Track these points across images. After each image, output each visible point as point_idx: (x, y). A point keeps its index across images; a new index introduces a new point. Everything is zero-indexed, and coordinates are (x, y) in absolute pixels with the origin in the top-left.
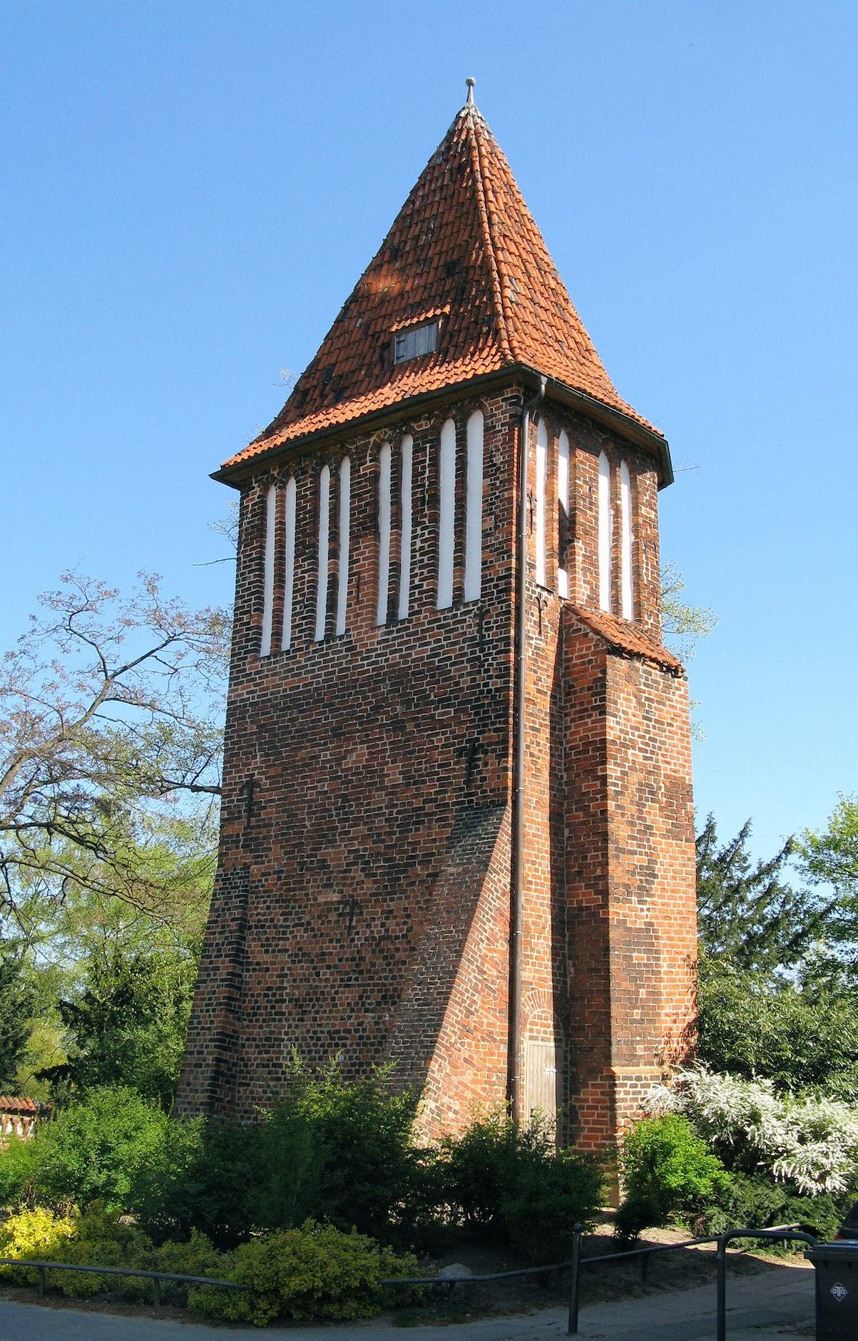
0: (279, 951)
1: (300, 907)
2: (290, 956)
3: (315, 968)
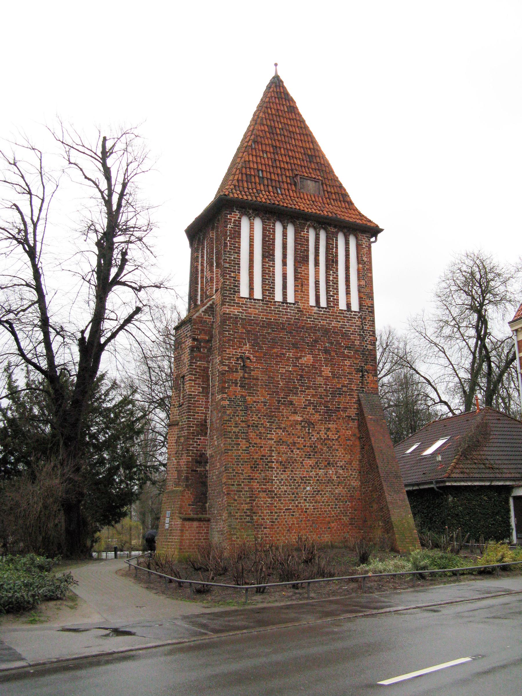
0: (268, 439)
3: (290, 449)
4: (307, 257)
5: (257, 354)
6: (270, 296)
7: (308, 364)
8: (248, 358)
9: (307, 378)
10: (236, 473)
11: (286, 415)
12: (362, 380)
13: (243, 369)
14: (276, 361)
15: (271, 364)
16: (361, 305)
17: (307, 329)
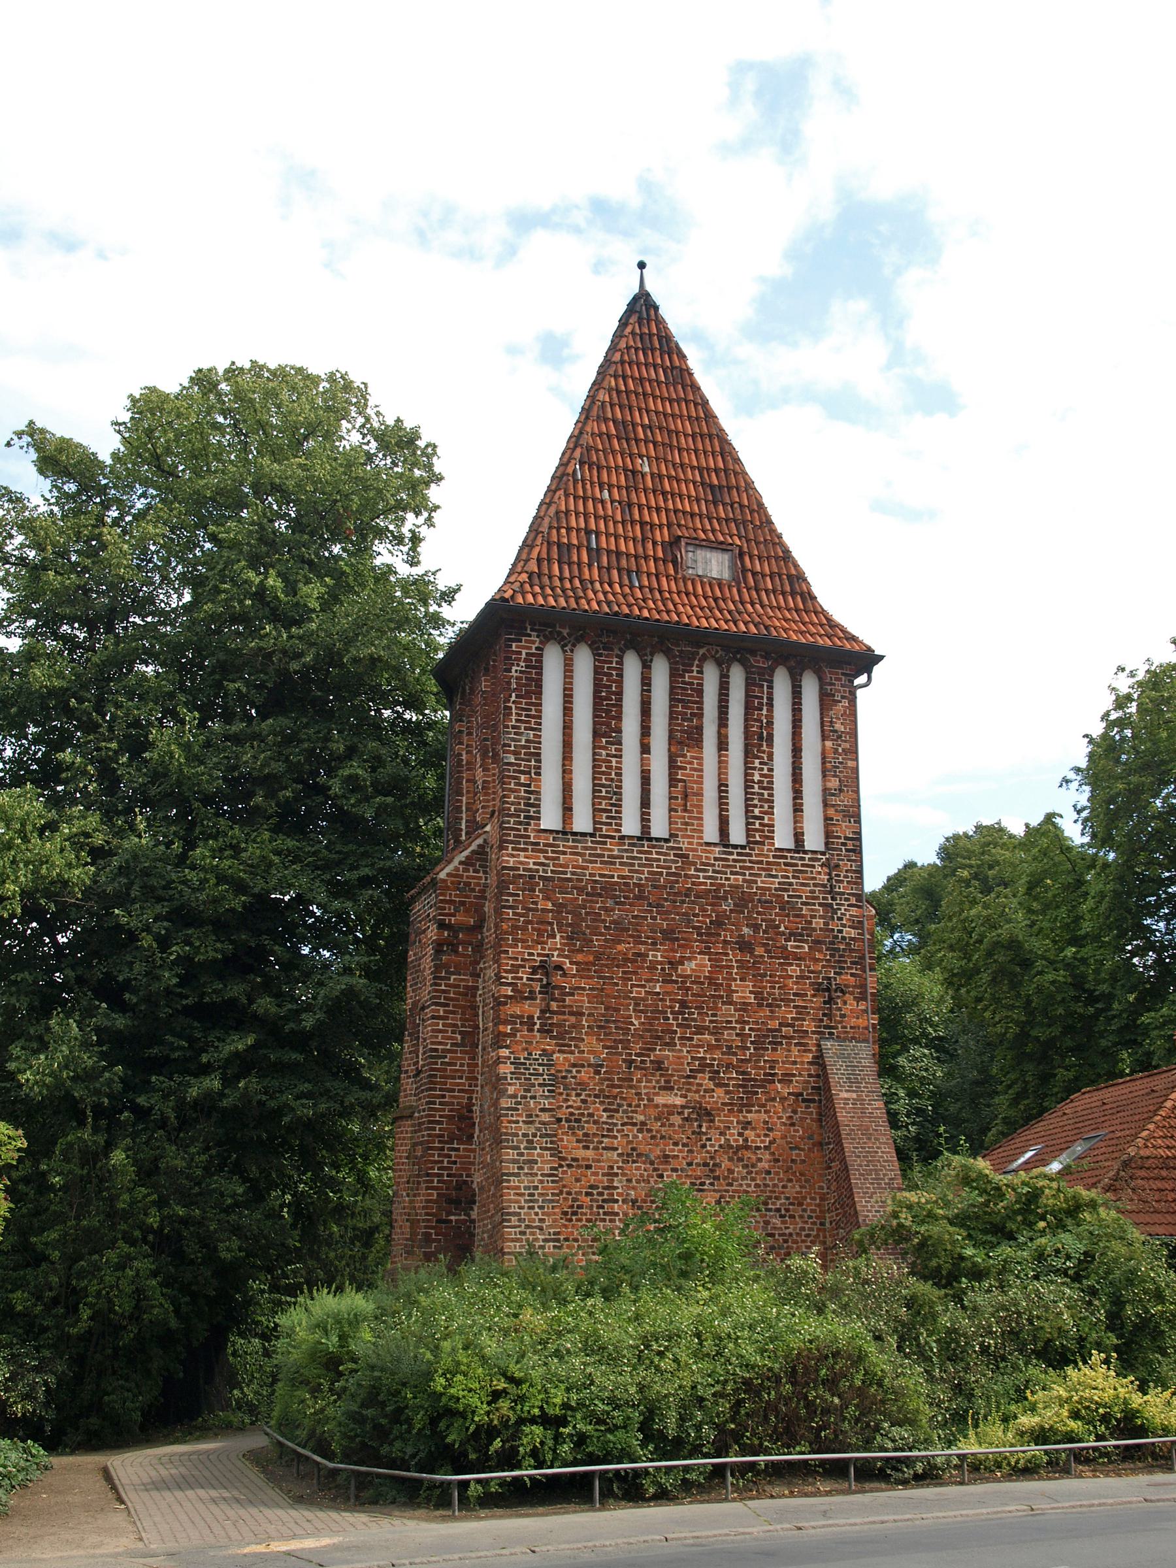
0: (604, 1148)
1: (630, 1105)
2: (619, 1155)
3: (655, 1170)
4: (700, 729)
5: (579, 957)
6: (610, 824)
7: (700, 977)
8: (559, 967)
9: (696, 1008)
10: (528, 1227)
11: (646, 1094)
12: (830, 1009)
13: (546, 993)
14: (624, 972)
15: (612, 978)
16: (828, 835)
17: (697, 896)
